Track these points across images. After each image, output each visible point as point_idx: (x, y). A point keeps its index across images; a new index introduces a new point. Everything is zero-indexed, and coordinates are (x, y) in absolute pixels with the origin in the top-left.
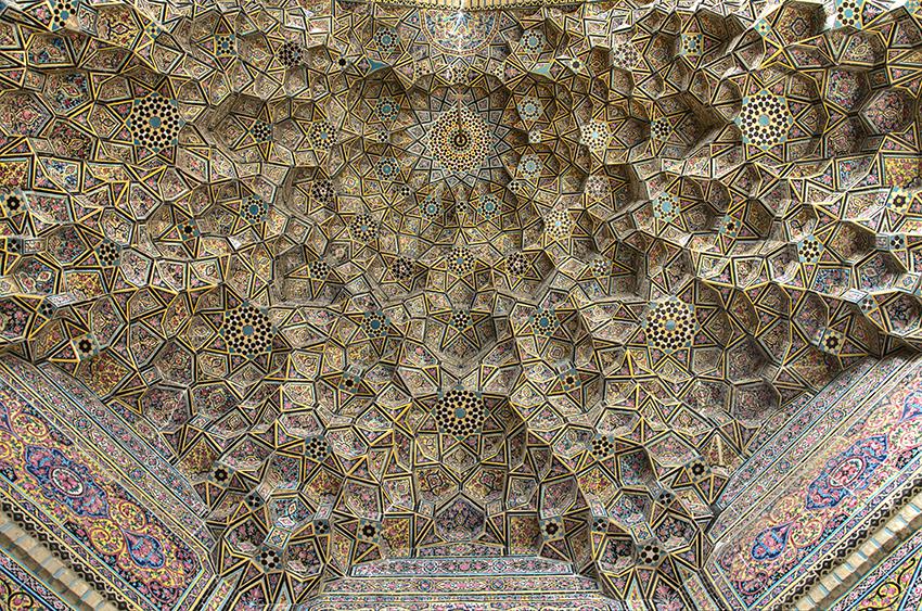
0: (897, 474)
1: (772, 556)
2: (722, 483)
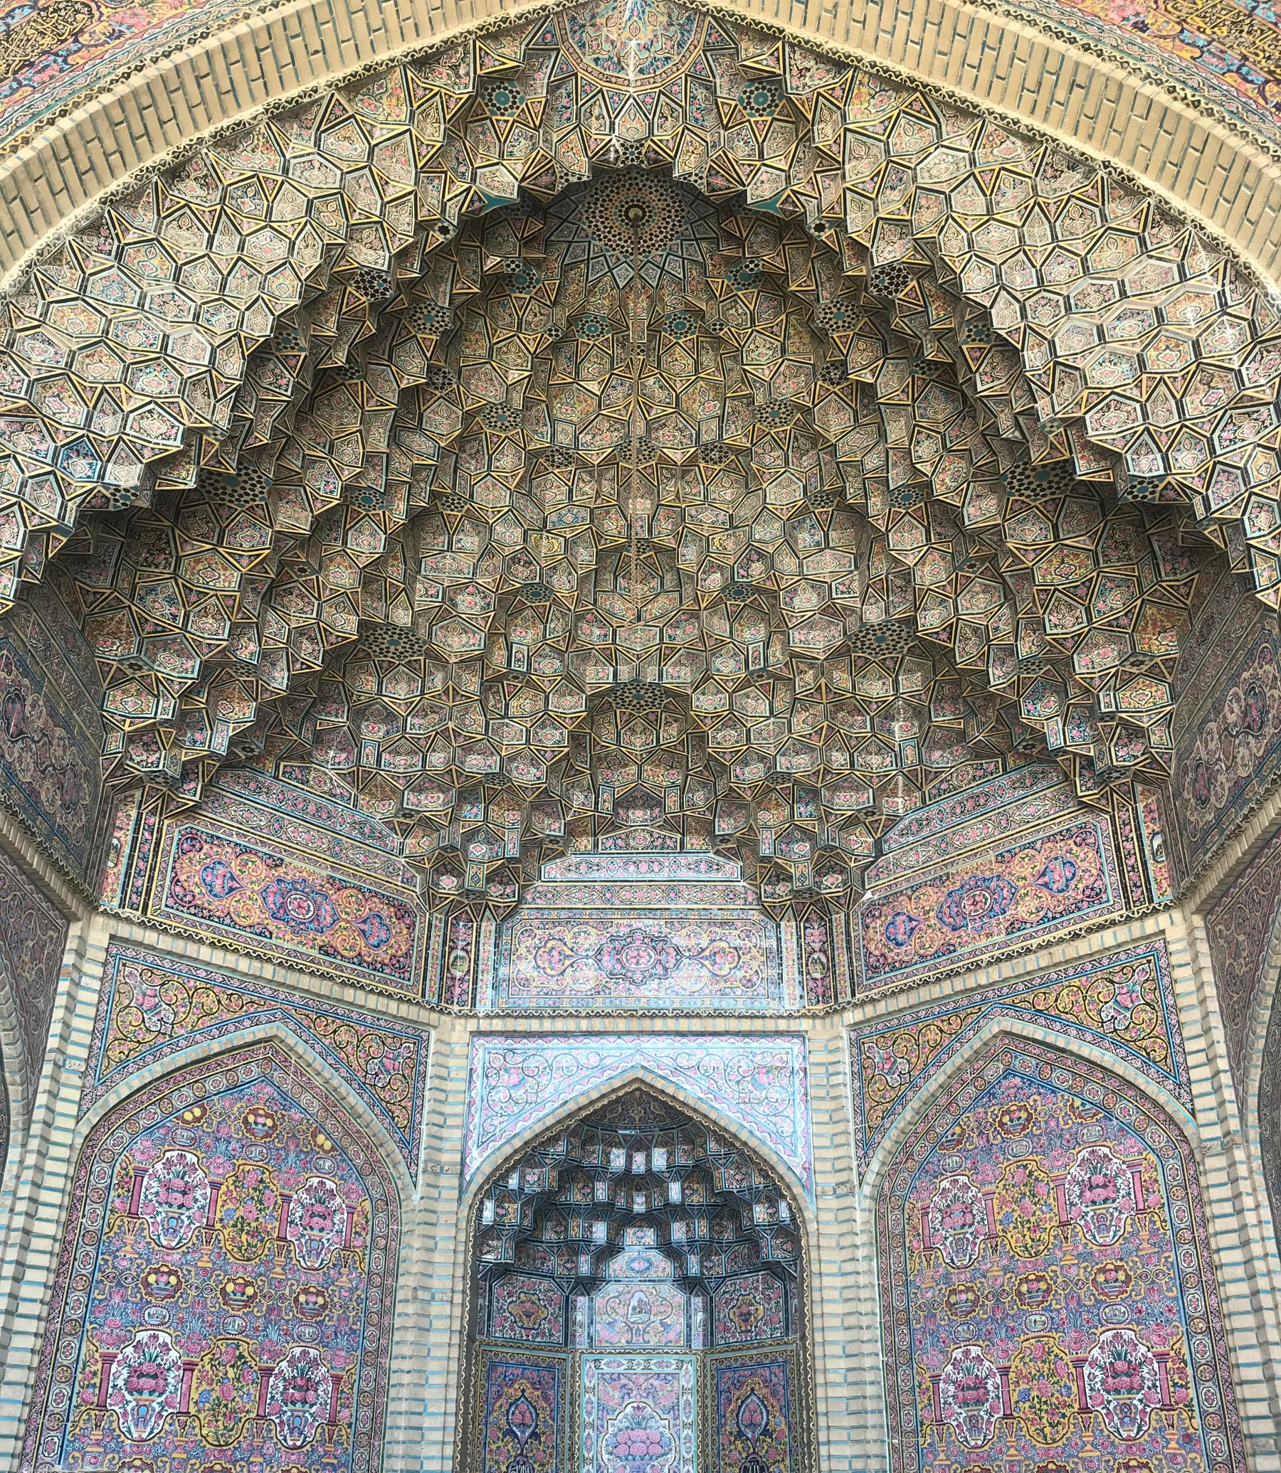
0: (1002, 937)
1: (897, 944)
2: (893, 820)
